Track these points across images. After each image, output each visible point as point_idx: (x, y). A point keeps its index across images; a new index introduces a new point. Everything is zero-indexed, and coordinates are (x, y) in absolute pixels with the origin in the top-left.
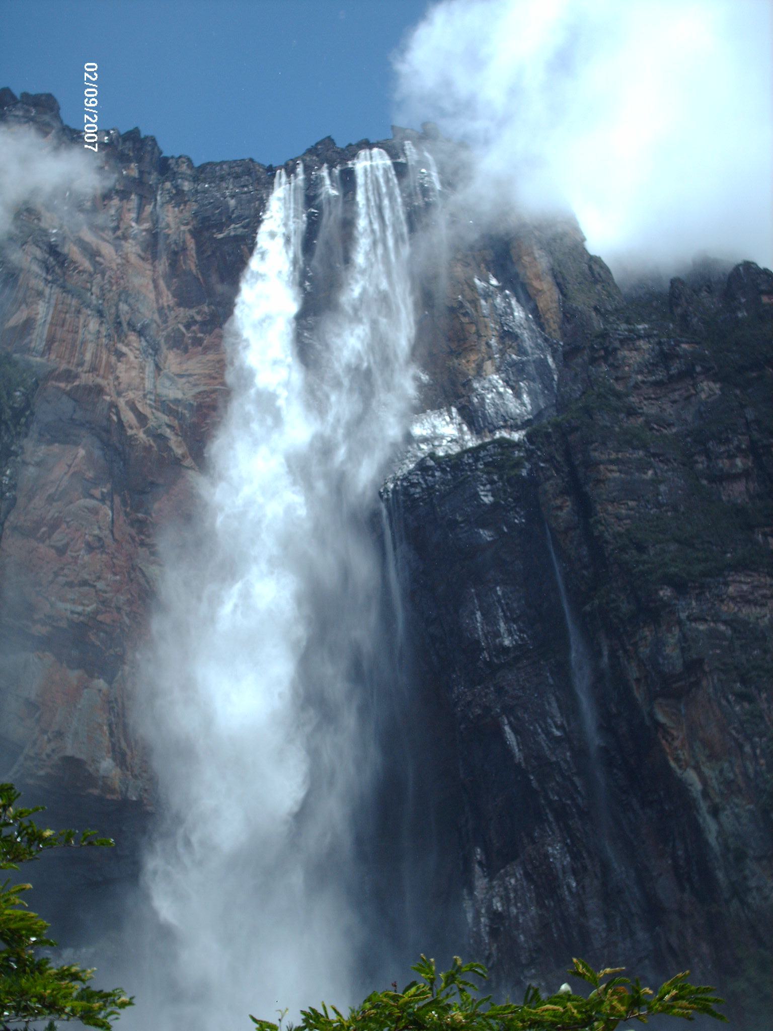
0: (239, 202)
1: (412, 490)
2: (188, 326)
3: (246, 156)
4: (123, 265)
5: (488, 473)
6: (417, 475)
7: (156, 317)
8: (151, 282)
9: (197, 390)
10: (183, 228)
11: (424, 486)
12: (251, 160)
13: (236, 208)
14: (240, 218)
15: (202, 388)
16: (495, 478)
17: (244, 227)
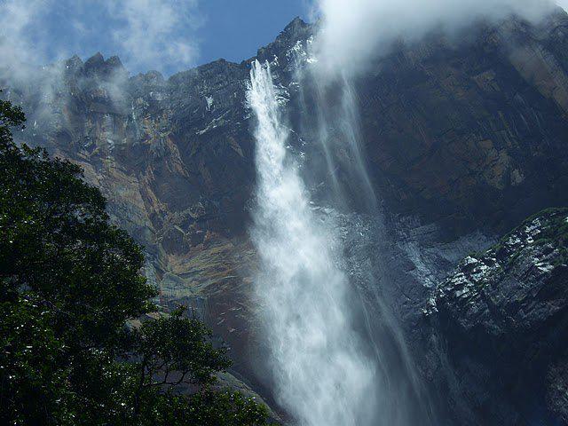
0: (216, 98)
1: (458, 294)
2: (184, 226)
3: (216, 59)
4: (104, 180)
5: (541, 244)
6: (461, 276)
7: (149, 223)
8: (138, 193)
9: (205, 285)
10: (162, 135)
11: (471, 285)
12: (222, 60)
13: (214, 103)
14: (219, 112)
15: (210, 282)
16: (550, 246)
17: (225, 118)
